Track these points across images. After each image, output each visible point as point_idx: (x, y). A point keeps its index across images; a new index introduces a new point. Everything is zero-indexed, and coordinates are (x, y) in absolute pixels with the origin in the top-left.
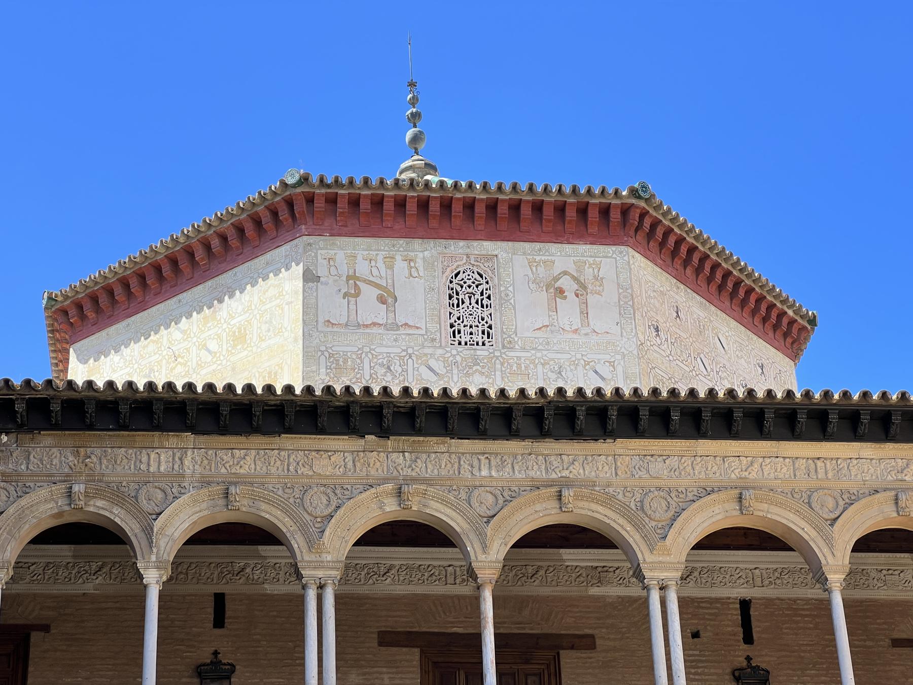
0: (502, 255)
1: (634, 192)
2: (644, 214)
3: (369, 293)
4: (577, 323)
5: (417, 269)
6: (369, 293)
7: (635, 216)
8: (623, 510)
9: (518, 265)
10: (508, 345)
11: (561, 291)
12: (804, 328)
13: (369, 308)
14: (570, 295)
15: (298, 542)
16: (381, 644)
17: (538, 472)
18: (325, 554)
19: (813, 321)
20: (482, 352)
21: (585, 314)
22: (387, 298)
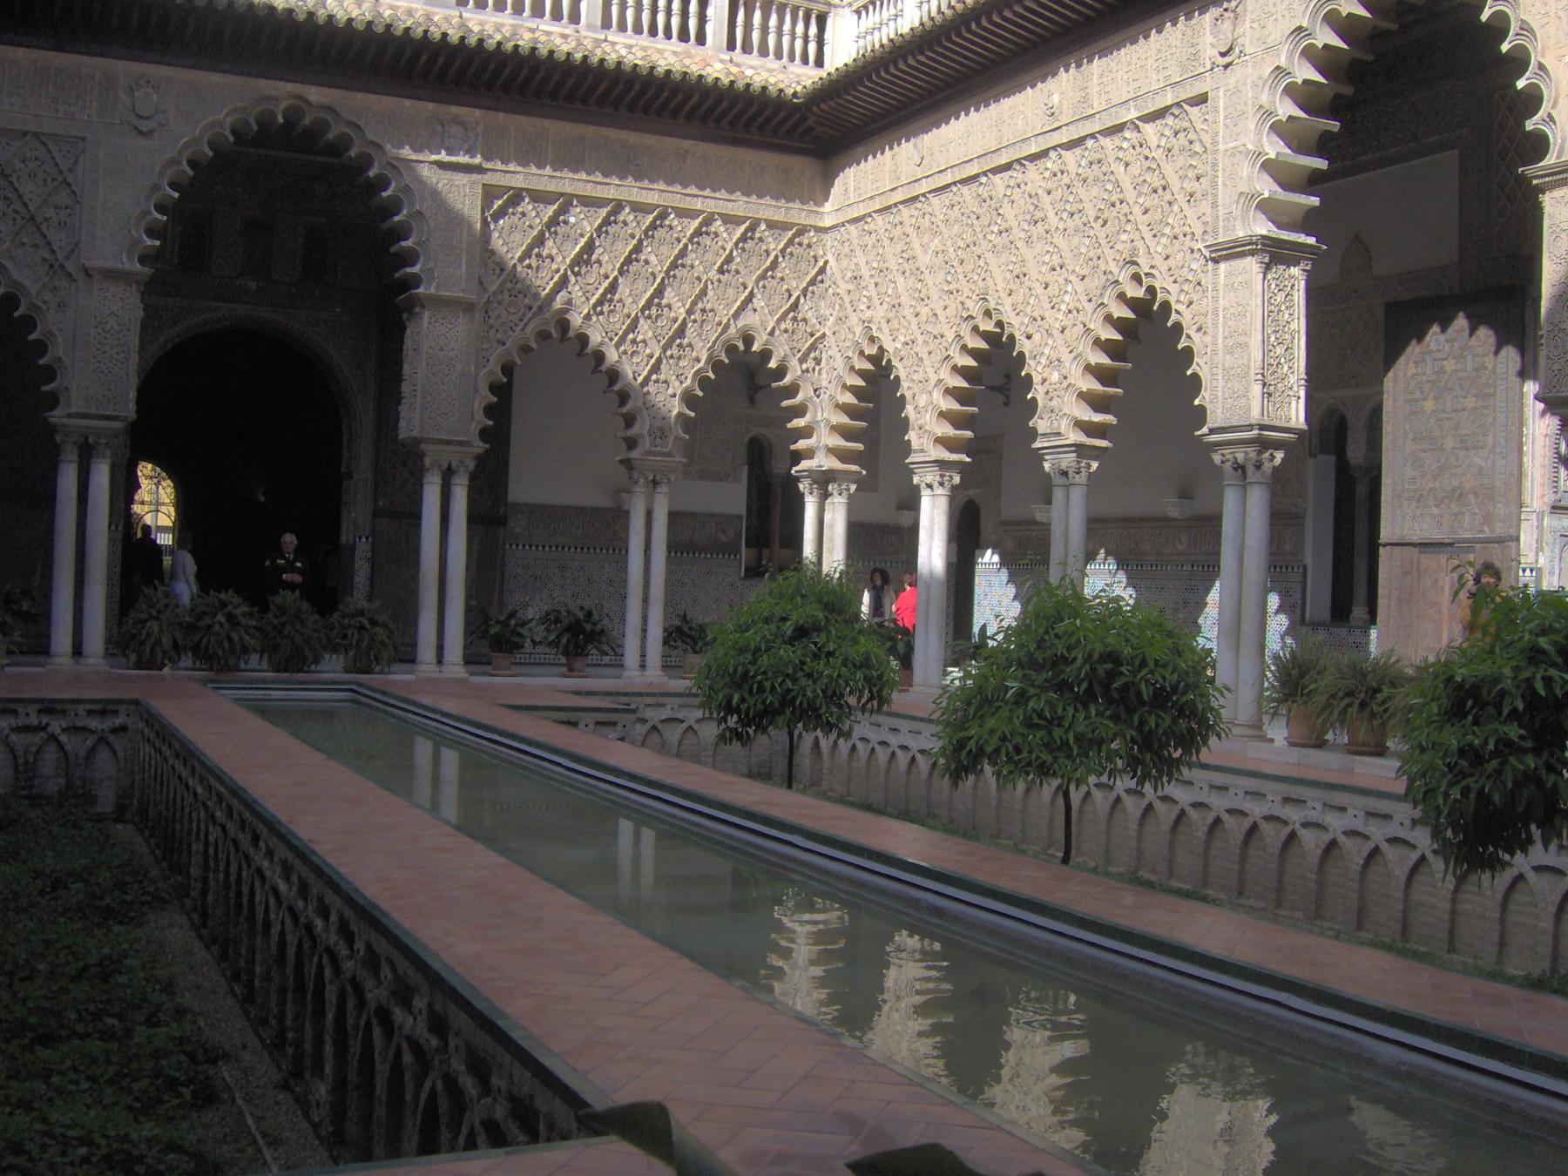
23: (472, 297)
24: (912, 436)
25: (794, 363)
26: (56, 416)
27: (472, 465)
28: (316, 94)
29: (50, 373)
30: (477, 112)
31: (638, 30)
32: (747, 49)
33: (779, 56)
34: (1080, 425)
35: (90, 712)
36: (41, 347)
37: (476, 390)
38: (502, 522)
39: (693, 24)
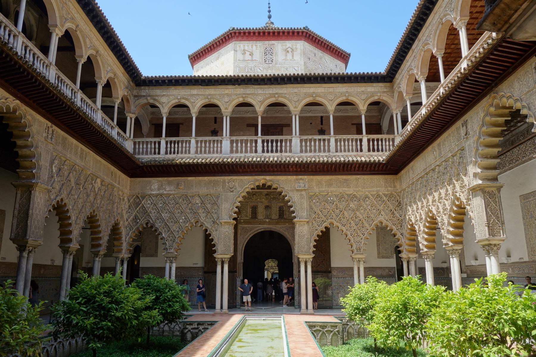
0: (276, 44)
1: (304, 28)
2: (307, 33)
3: (248, 53)
4: (291, 58)
5: (257, 48)
6: (248, 53)
7: (304, 34)
8: (288, 99)
9: (279, 46)
10: (276, 64)
11: (288, 51)
12: (347, 57)
13: (248, 57)
14: (290, 52)
15: (222, 108)
16: (247, 126)
17: (271, 92)
18: (227, 109)
19: (349, 55)
20: (271, 65)
21: (293, 56)
22: (251, 54)
23: (307, 220)
24: (420, 245)
25: (394, 227)
26: (215, 255)
27: (311, 260)
28: (268, 178)
29: (214, 245)
30: (306, 177)
31: (345, 151)
32: (374, 150)
33: (382, 151)
34: (452, 241)
35: (208, 324)
36: (212, 240)
37: (311, 242)
38: (330, 272)
39: (359, 147)
